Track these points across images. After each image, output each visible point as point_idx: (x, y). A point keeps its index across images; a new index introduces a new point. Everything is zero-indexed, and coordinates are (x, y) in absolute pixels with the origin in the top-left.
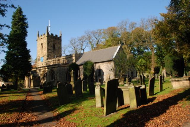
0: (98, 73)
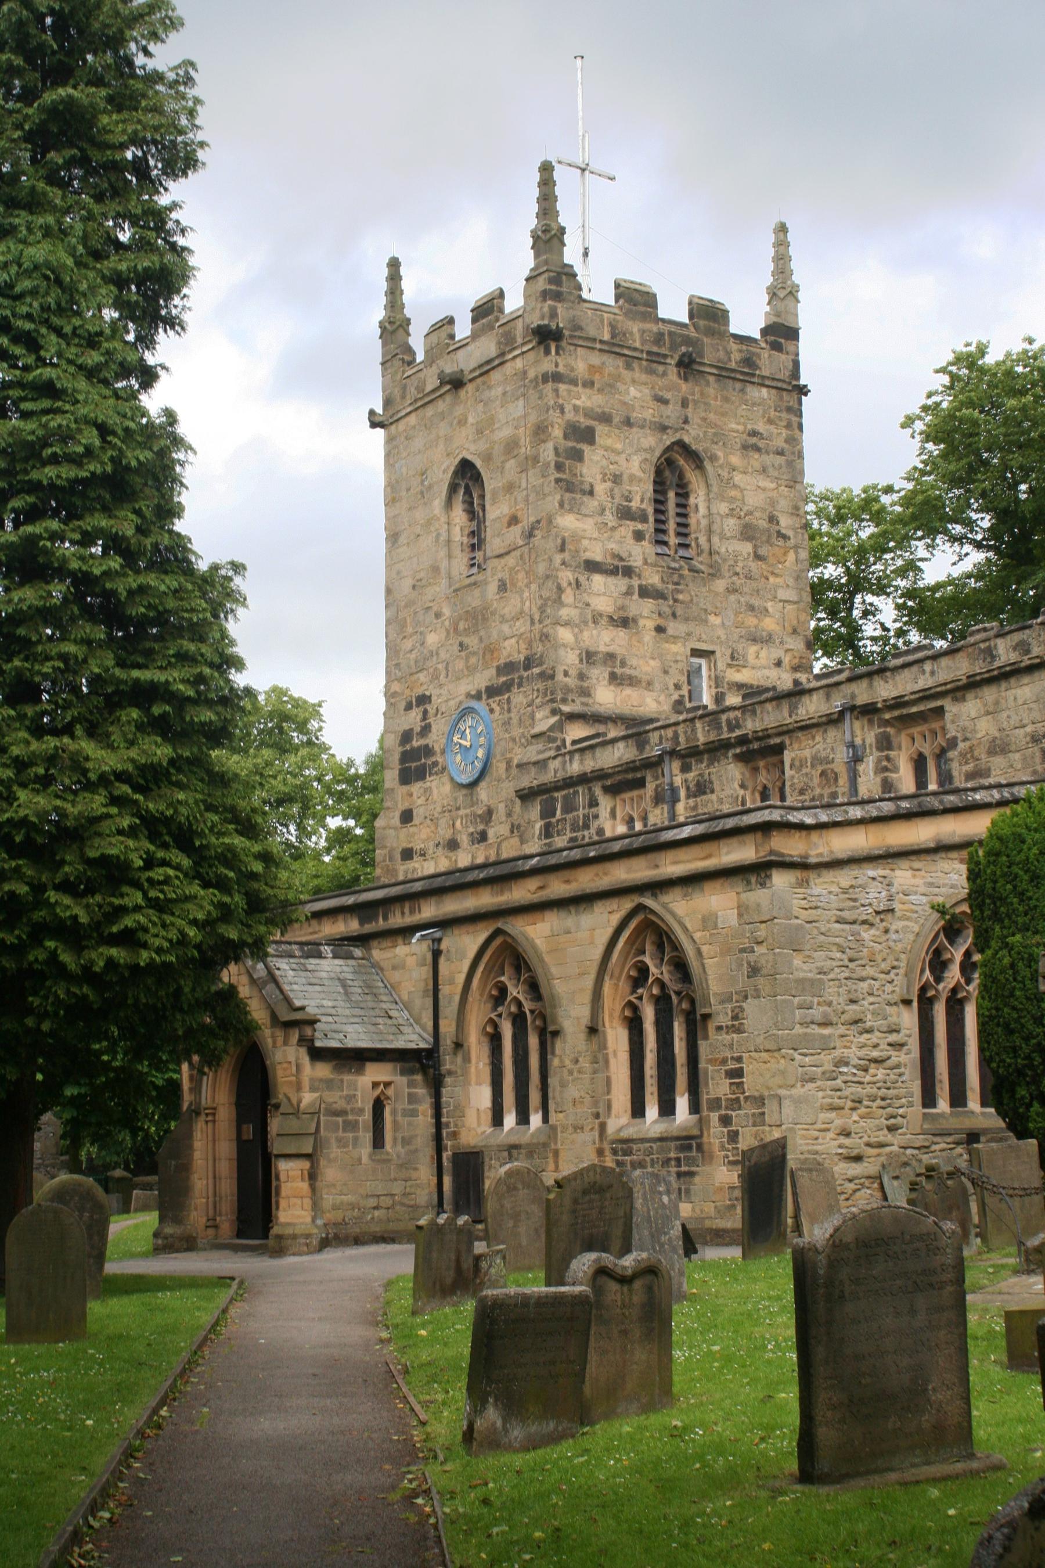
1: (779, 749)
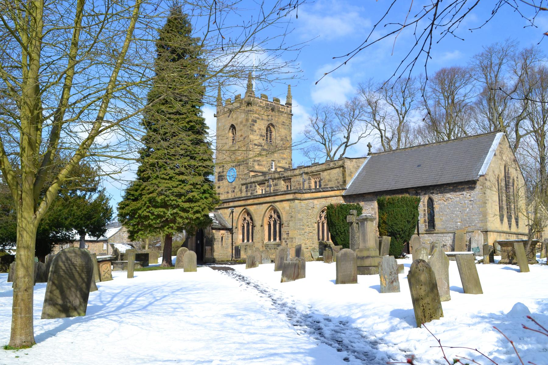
0: (425, 222)
1: (290, 179)
